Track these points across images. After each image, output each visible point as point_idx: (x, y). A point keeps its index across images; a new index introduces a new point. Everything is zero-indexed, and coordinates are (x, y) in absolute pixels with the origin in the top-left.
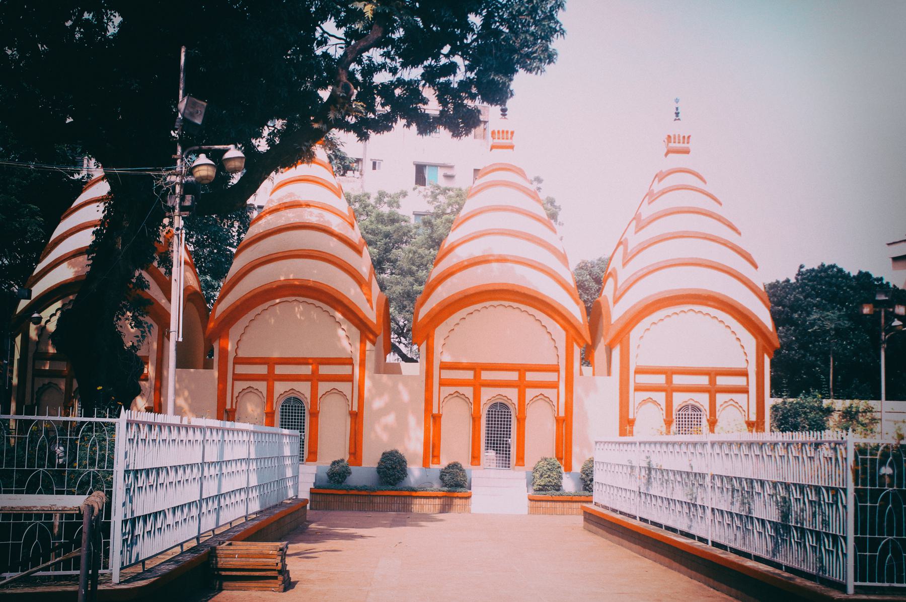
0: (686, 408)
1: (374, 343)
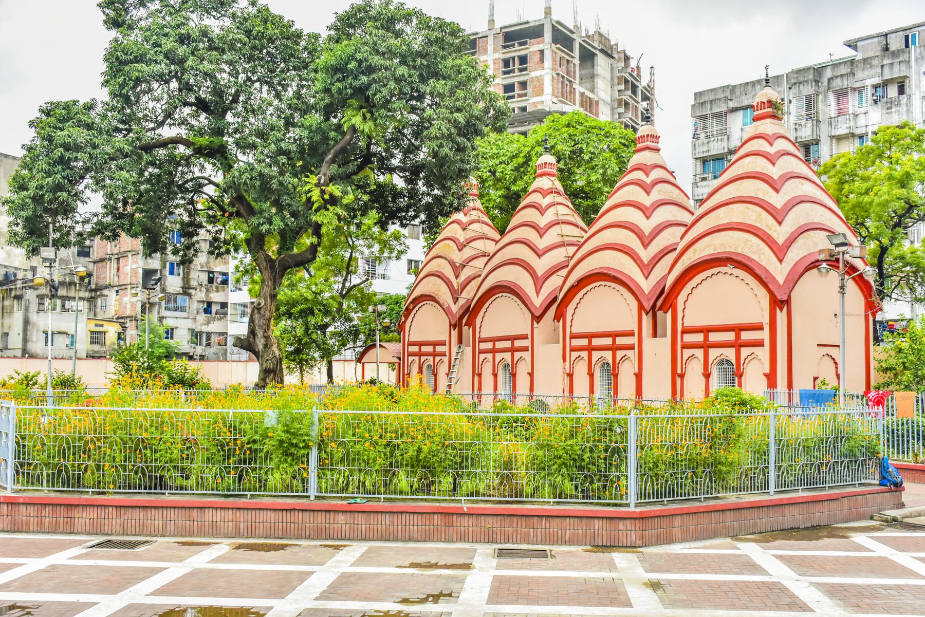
0: (721, 363)
1: (538, 323)
